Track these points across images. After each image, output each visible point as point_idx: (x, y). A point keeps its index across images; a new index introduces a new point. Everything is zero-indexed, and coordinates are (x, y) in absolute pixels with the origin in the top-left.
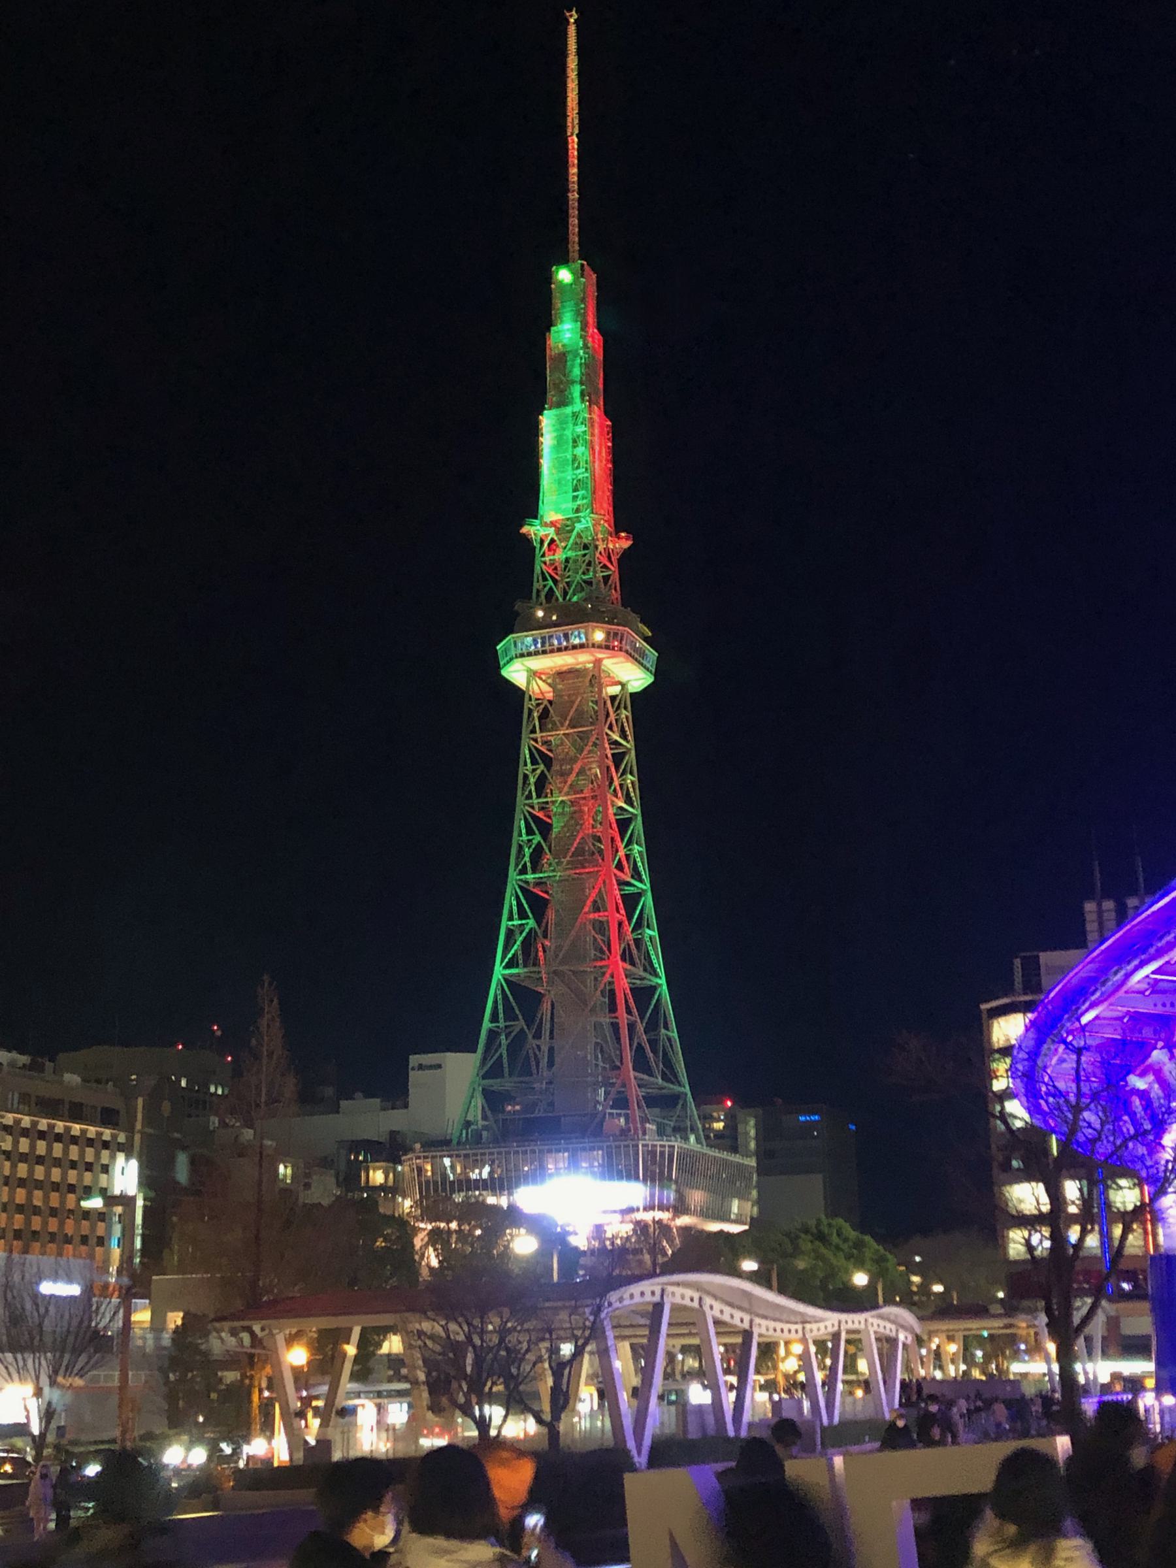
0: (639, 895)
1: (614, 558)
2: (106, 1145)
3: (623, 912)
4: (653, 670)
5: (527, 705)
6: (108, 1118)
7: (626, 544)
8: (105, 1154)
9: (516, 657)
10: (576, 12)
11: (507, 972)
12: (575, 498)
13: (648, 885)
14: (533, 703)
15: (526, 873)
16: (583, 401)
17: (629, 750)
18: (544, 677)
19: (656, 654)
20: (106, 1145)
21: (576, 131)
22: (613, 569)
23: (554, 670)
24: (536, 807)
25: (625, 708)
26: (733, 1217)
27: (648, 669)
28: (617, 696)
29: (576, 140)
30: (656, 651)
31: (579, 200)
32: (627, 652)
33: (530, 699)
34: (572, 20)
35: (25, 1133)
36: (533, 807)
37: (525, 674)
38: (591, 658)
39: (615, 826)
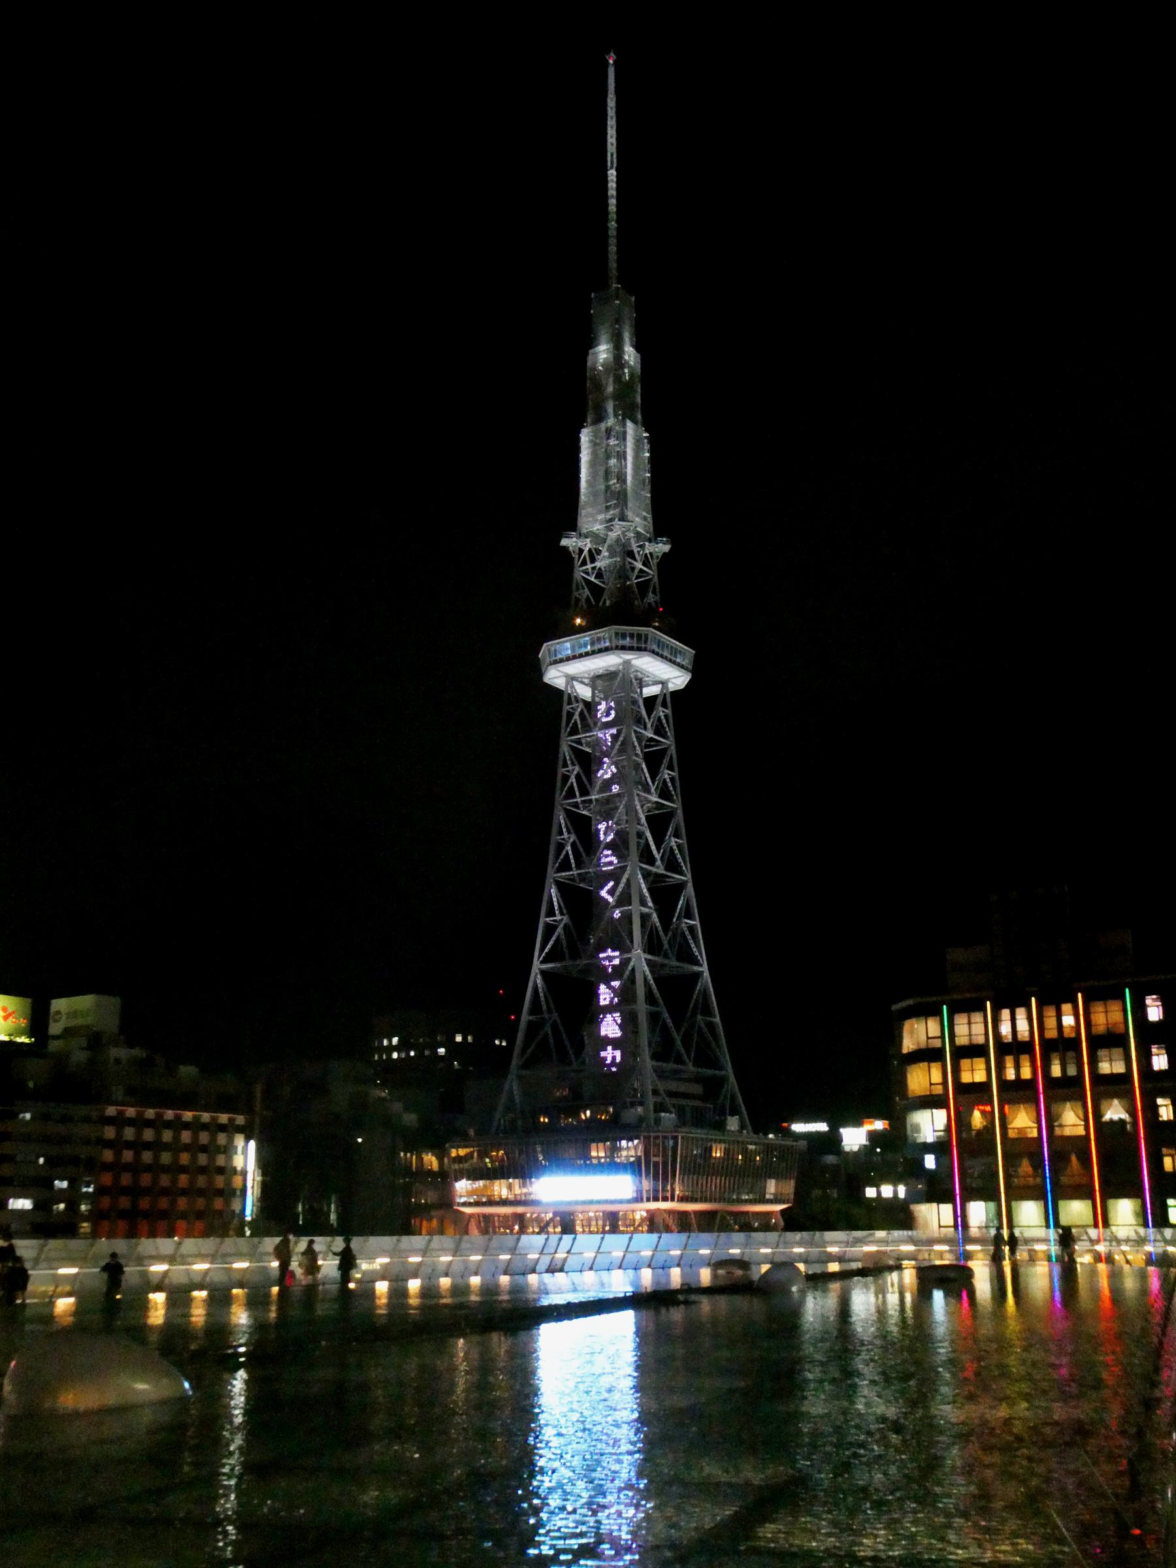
0: (681, 886)
1: (654, 563)
2: (223, 1128)
3: (650, 904)
4: (690, 667)
5: (566, 708)
6: (225, 1103)
7: (667, 548)
8: (222, 1139)
9: (551, 664)
10: (614, 53)
11: (544, 966)
12: (608, 508)
13: (689, 875)
14: (574, 705)
15: (571, 869)
16: (616, 416)
17: (670, 746)
18: (586, 681)
19: (694, 652)
20: (223, 1128)
21: (615, 165)
22: (652, 573)
23: (592, 674)
24: (581, 806)
25: (664, 705)
26: (768, 1196)
27: (682, 667)
28: (655, 698)
29: (615, 173)
30: (693, 649)
31: (618, 229)
32: (653, 652)
33: (570, 703)
34: (611, 62)
35: (131, 1122)
36: (578, 808)
37: (564, 678)
38: (621, 661)
39: (643, 820)
